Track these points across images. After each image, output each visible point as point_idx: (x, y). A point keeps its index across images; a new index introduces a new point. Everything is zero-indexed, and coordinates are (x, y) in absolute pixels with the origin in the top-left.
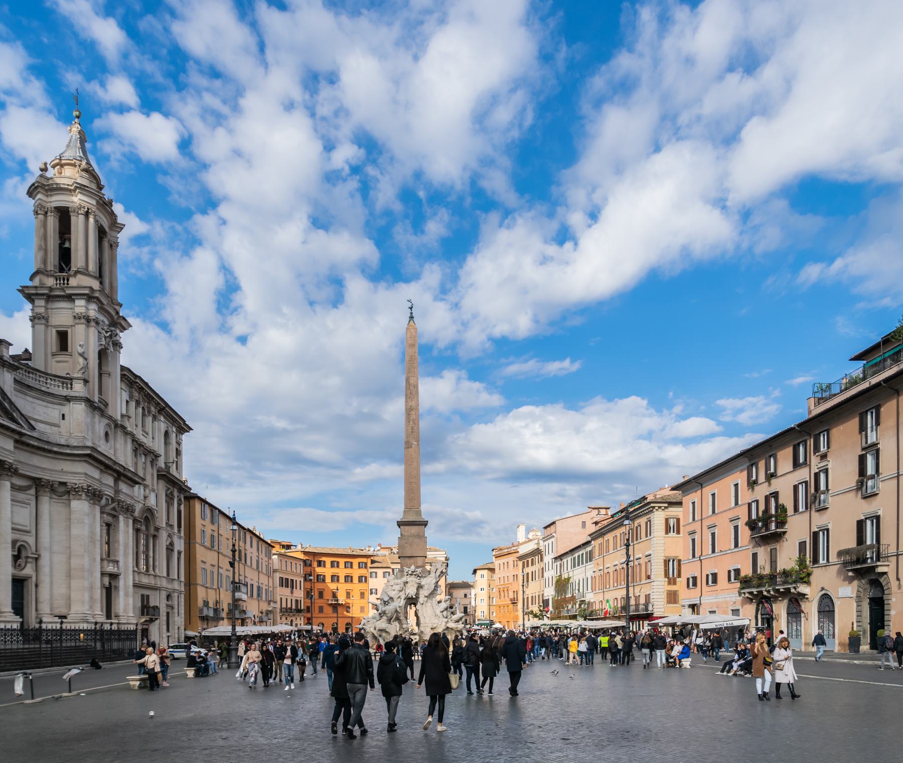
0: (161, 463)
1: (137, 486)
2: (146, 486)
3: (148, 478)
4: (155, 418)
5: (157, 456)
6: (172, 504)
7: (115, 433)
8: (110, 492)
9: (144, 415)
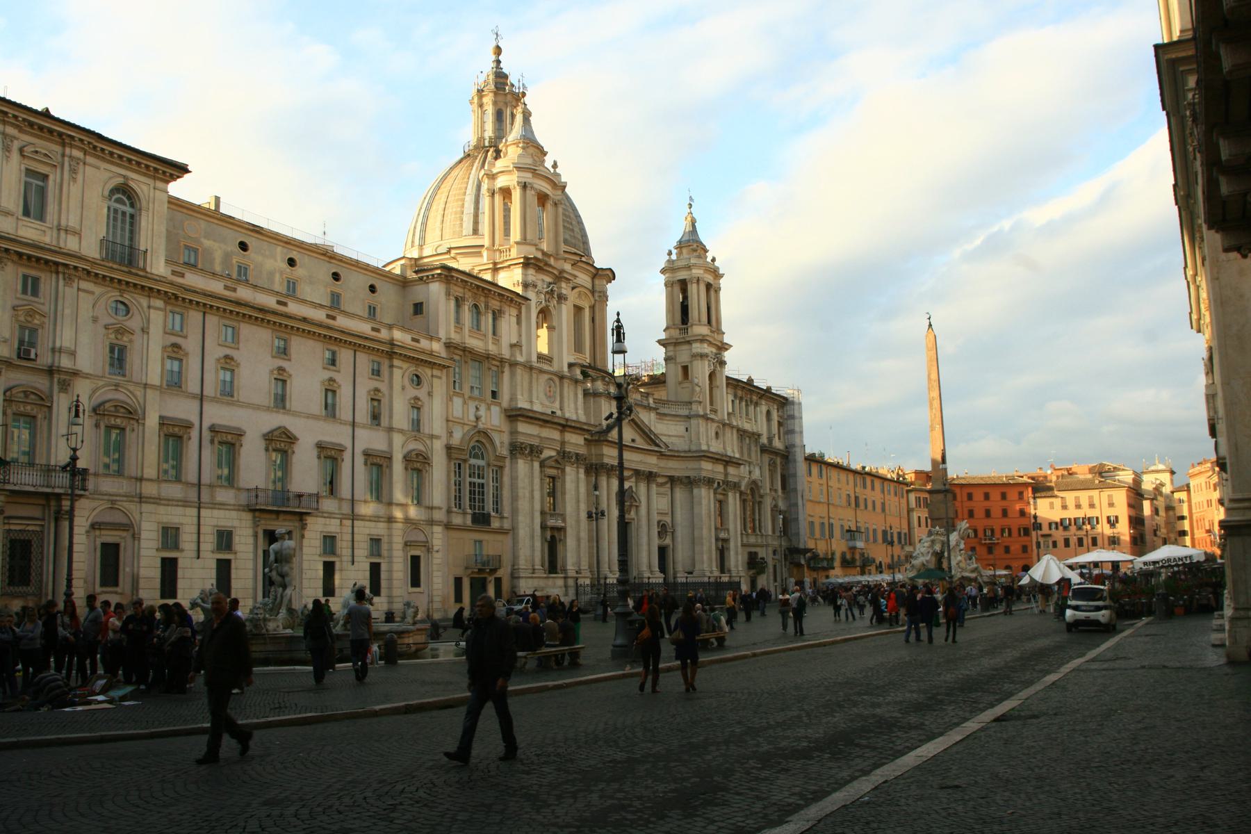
0: (764, 440)
2: (750, 463)
3: (753, 455)
5: (759, 435)
6: (775, 471)
8: (721, 477)
9: (747, 405)
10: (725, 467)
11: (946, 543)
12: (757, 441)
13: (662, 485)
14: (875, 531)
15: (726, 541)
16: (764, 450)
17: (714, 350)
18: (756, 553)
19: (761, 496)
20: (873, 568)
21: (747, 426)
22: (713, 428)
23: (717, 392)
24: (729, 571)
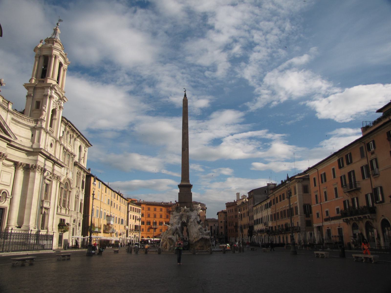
0: (76, 159)
1: (63, 168)
3: (70, 165)
4: (75, 139)
5: (74, 156)
7: (56, 144)
10: (53, 165)
11: (189, 218)
12: (73, 158)
13: (8, 166)
14: (116, 218)
15: (47, 209)
16: (76, 164)
17: (58, 98)
18: (64, 220)
19: (71, 188)
20: (114, 234)
21: (69, 148)
22: (50, 140)
23: (55, 123)
24: (47, 228)
